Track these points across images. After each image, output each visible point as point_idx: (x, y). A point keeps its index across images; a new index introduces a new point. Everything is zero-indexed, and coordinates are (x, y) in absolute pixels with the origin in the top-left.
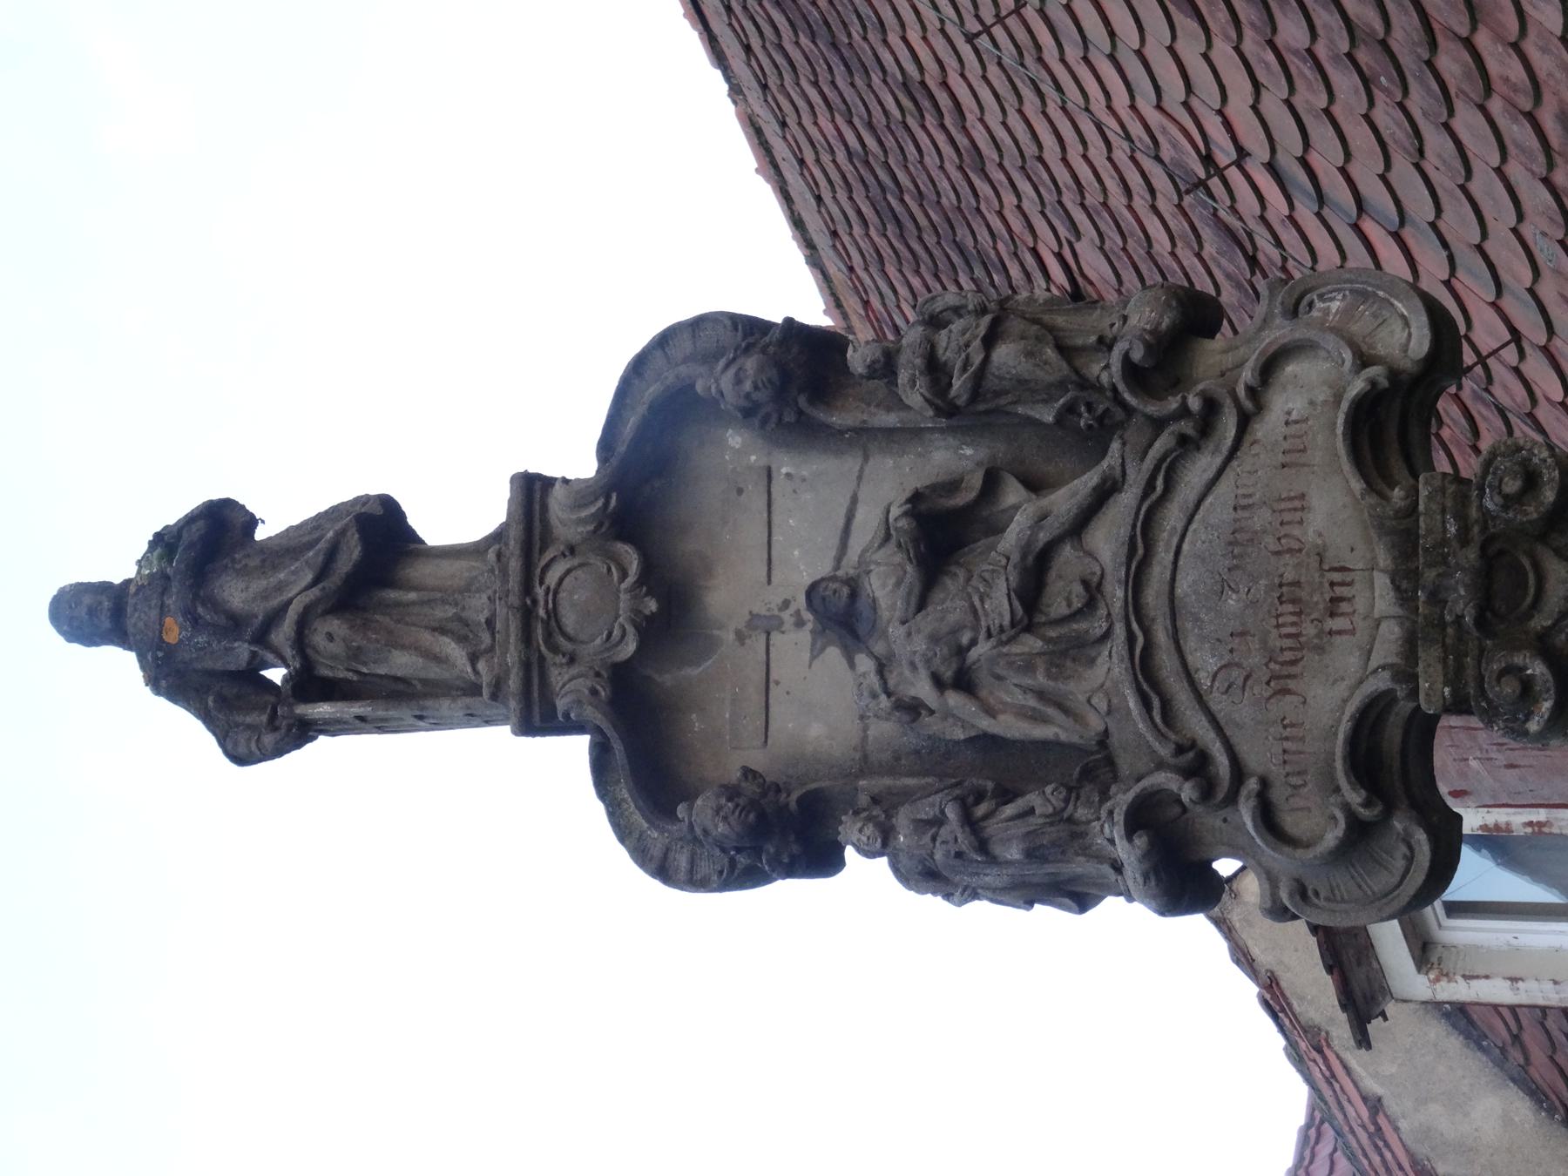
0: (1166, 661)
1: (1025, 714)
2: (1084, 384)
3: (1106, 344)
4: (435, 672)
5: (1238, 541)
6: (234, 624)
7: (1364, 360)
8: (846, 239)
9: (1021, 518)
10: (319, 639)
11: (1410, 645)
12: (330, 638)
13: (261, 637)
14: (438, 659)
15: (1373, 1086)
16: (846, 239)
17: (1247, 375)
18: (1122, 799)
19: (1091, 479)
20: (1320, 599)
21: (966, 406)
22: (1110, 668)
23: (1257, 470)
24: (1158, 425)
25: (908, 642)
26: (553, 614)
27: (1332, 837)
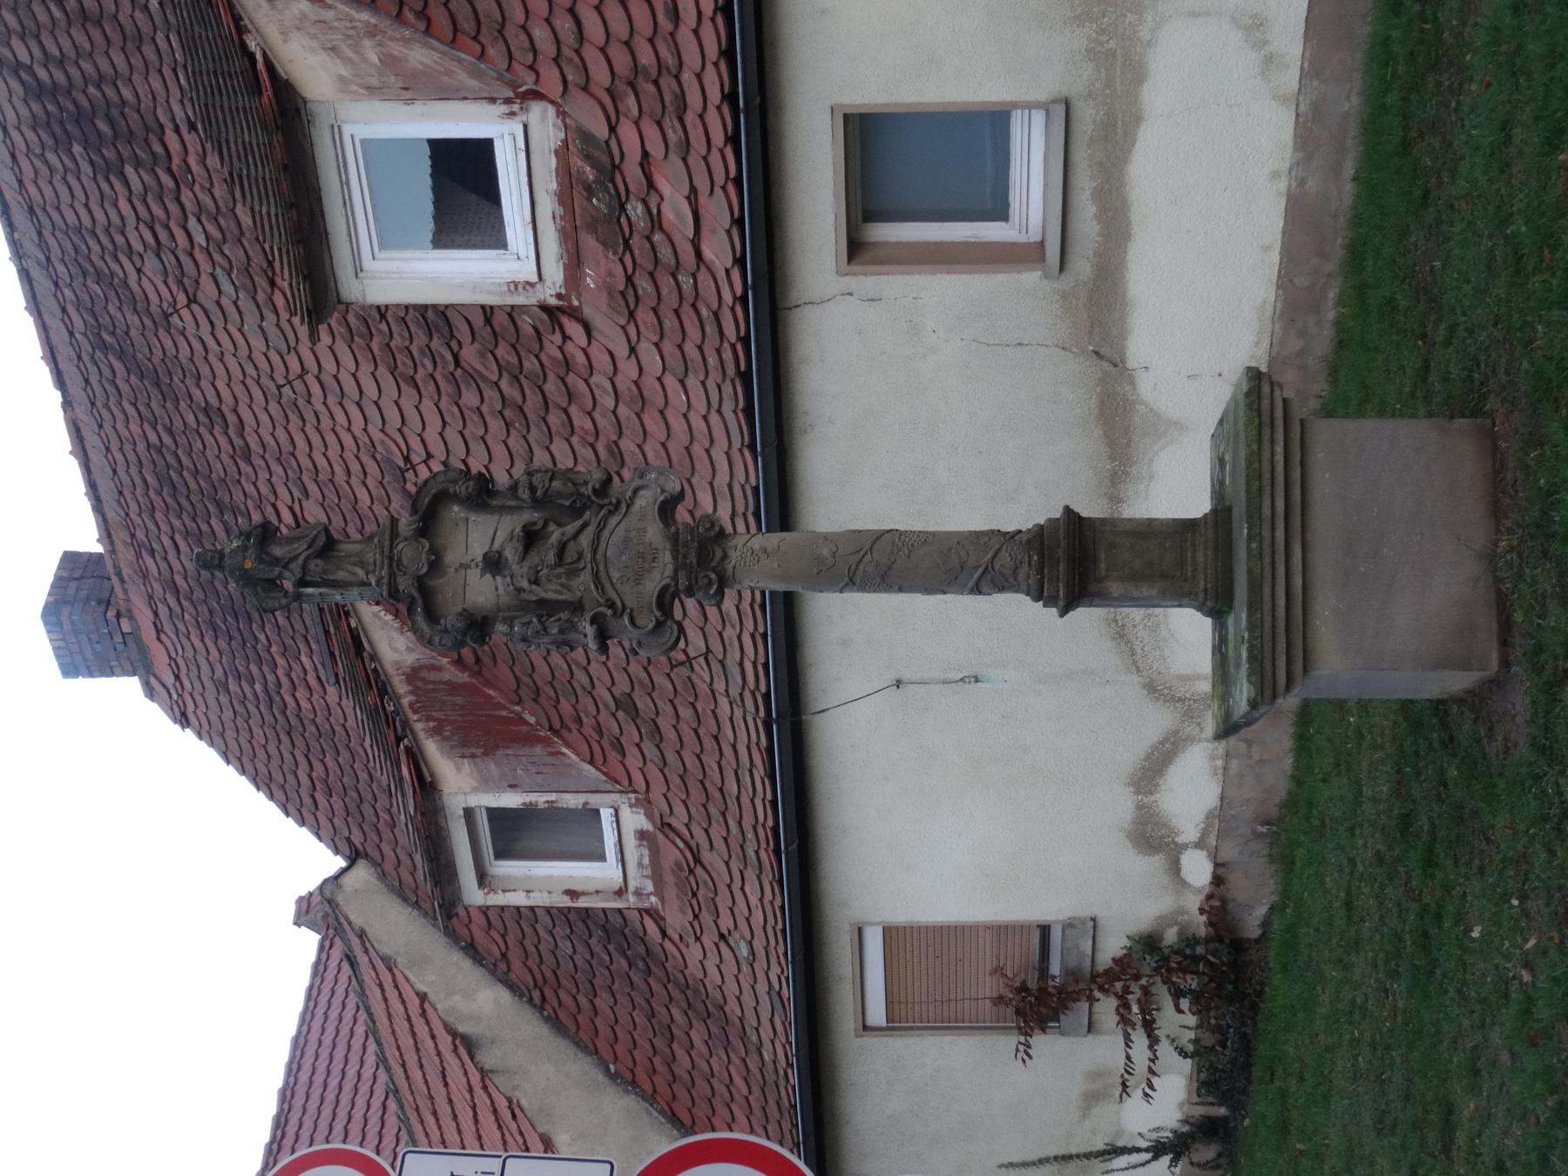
0: (603, 575)
1: (558, 592)
2: (579, 494)
3: (586, 483)
4: (352, 579)
5: (626, 541)
6: (276, 561)
7: (663, 491)
8: (128, 496)
9: (555, 535)
10: (312, 566)
11: (676, 571)
12: (316, 565)
13: (285, 567)
14: (354, 574)
15: (422, 988)
16: (128, 496)
17: (629, 493)
18: (588, 616)
19: (580, 522)
20: (650, 558)
21: (537, 503)
22: (585, 577)
23: (632, 521)
24: (602, 507)
25: (520, 571)
26: (400, 559)
27: (651, 625)
